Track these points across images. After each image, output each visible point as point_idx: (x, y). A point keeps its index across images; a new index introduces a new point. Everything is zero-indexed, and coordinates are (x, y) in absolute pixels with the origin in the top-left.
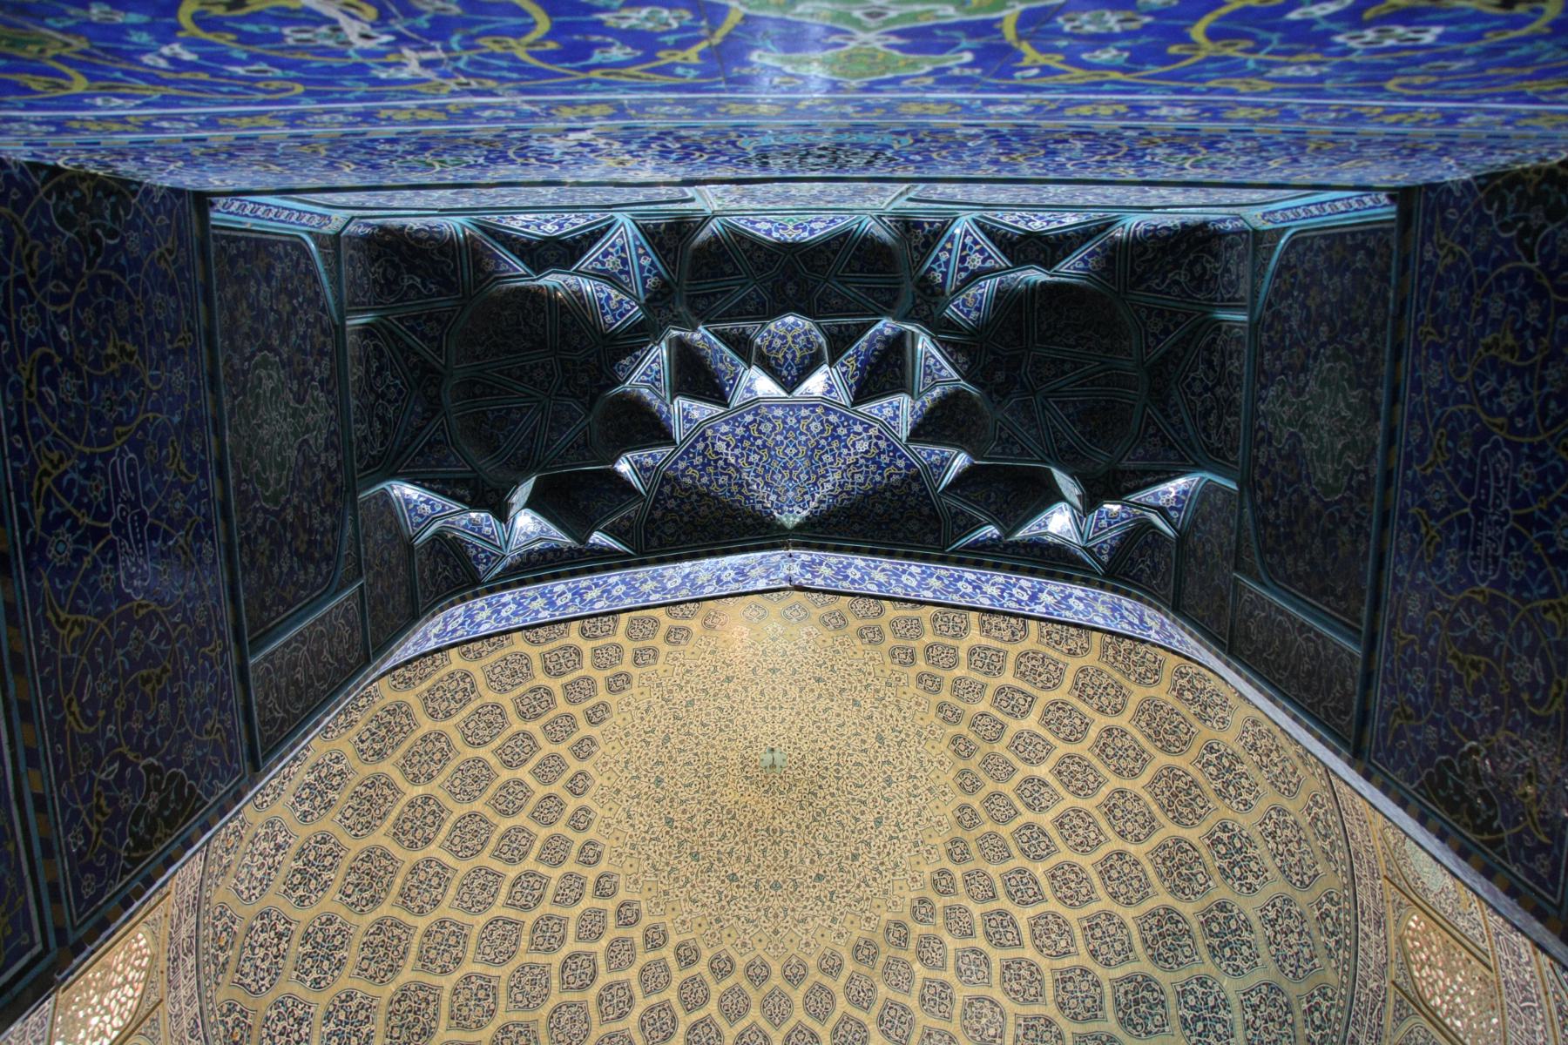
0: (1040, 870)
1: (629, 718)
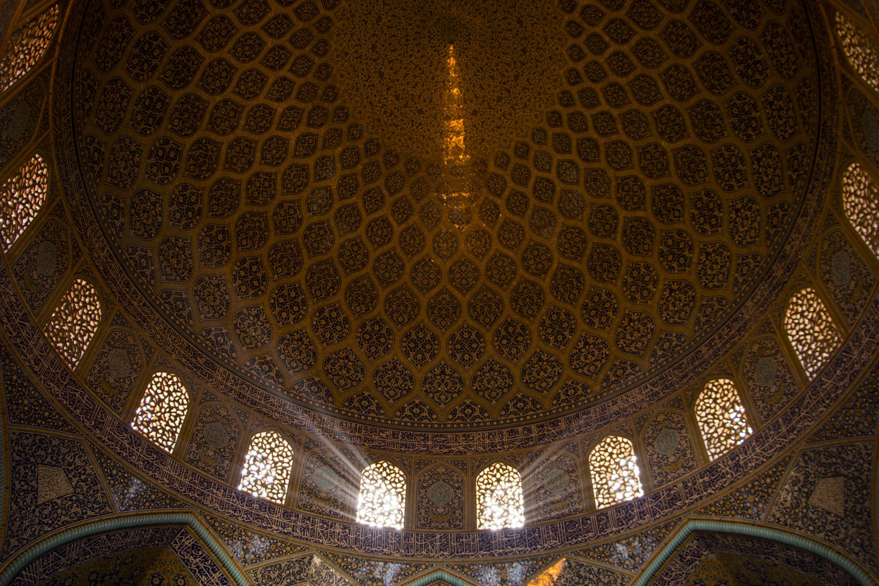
0: (270, 43)
1: (537, 106)
